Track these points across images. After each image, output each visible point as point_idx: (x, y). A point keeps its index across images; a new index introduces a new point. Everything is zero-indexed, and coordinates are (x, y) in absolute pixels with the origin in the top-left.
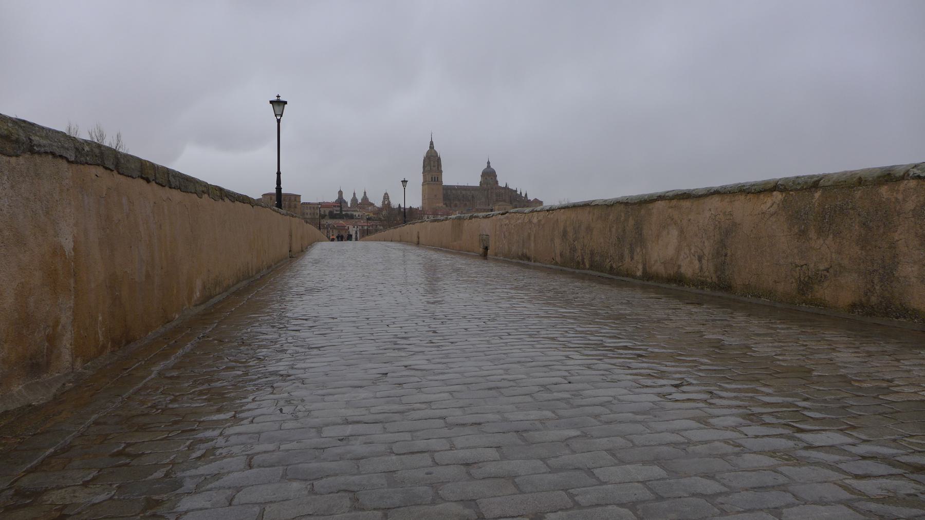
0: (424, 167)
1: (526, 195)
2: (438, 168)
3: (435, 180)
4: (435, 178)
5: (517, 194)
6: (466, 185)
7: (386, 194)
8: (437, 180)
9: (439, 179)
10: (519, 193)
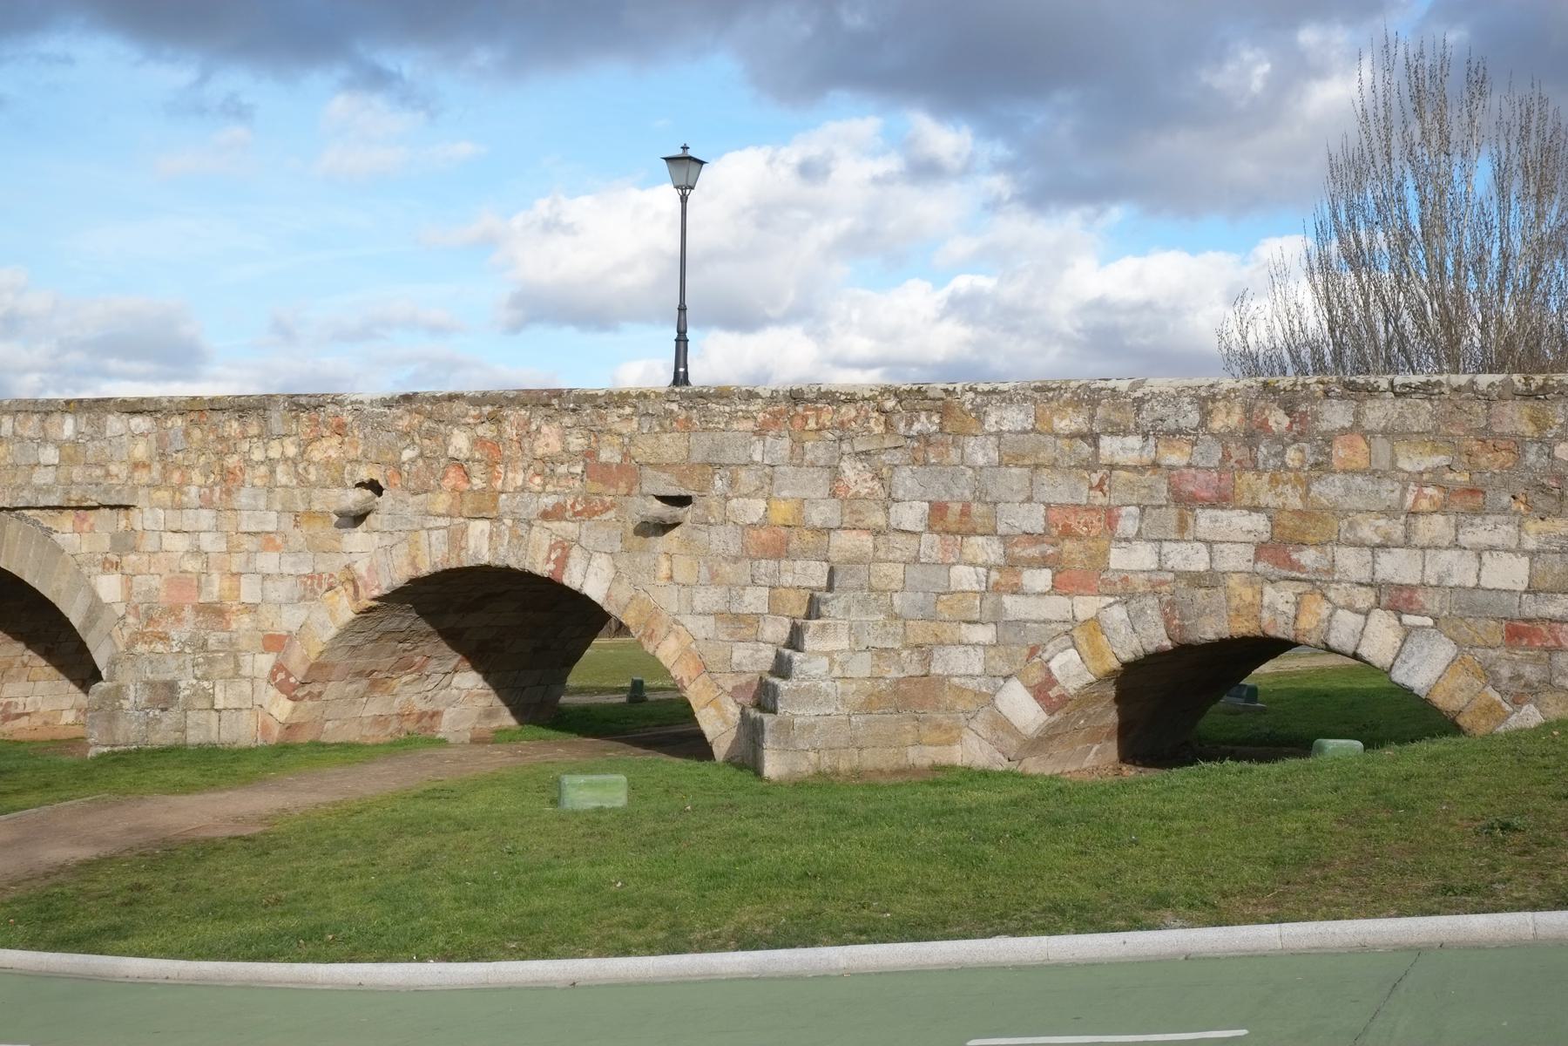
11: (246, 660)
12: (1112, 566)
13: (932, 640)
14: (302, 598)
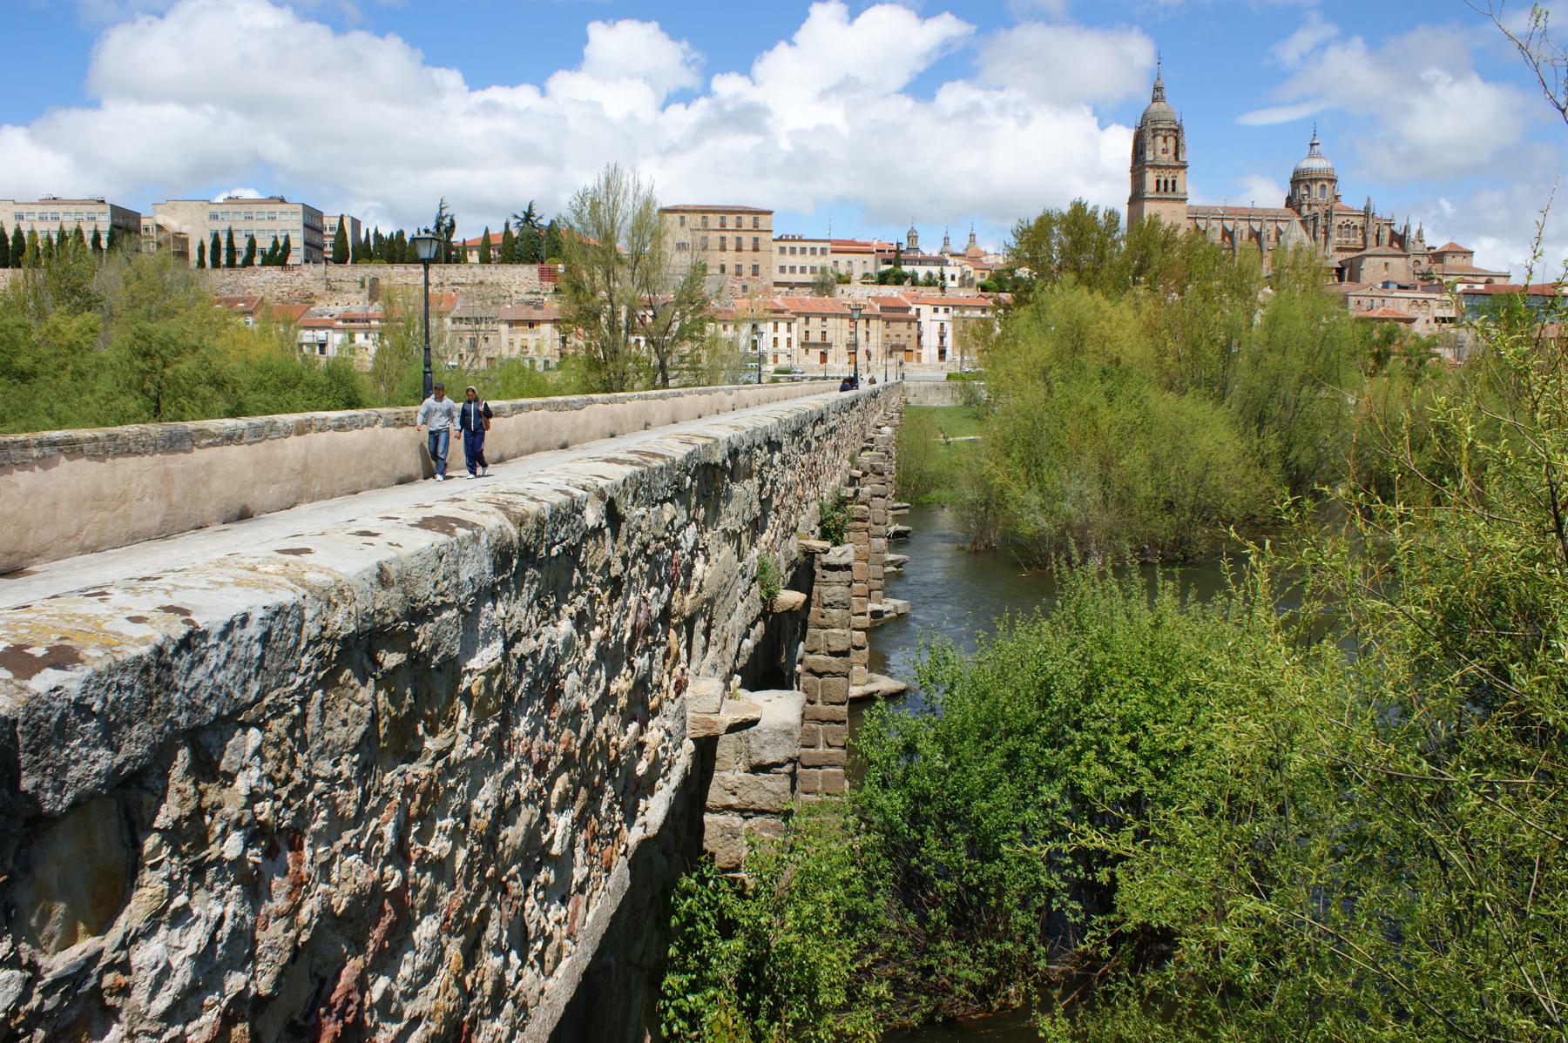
2: (1176, 154)
3: (1166, 190)
4: (1166, 182)
6: (1248, 205)
8: (1173, 190)
9: (1177, 185)
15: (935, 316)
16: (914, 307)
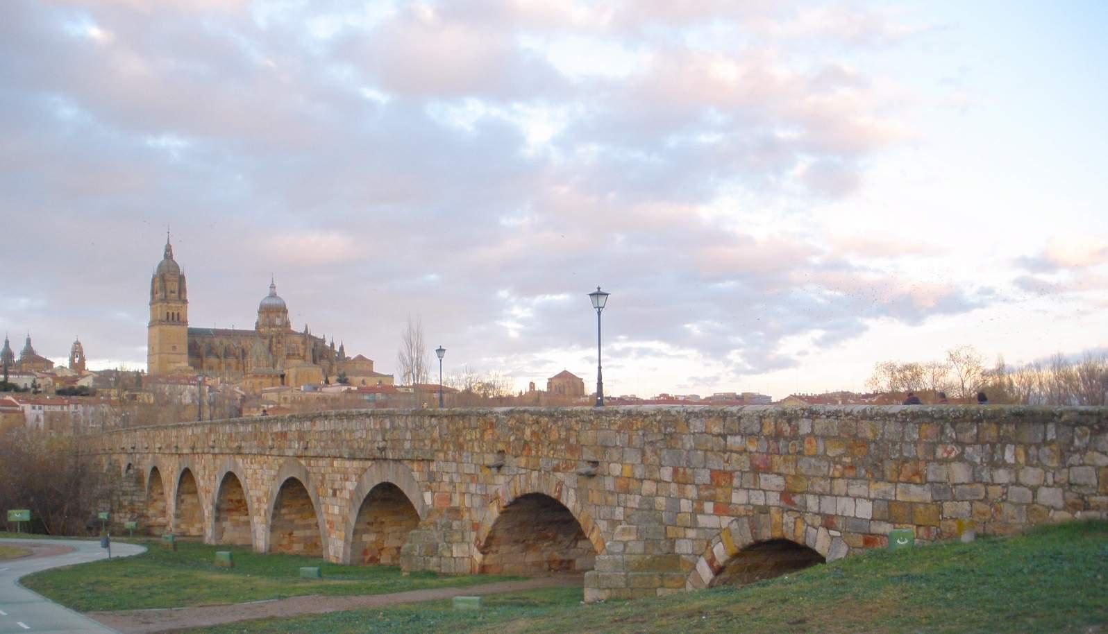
0: (153, 293)
1: (342, 348)
2: (180, 293)
3: (173, 319)
4: (173, 313)
5: (325, 347)
6: (230, 328)
7: (78, 343)
8: (178, 319)
10: (328, 344)
11: (467, 534)
12: (733, 501)
13: (675, 536)
14: (483, 506)
15: (33, 411)
16: (22, 405)
